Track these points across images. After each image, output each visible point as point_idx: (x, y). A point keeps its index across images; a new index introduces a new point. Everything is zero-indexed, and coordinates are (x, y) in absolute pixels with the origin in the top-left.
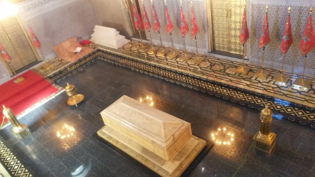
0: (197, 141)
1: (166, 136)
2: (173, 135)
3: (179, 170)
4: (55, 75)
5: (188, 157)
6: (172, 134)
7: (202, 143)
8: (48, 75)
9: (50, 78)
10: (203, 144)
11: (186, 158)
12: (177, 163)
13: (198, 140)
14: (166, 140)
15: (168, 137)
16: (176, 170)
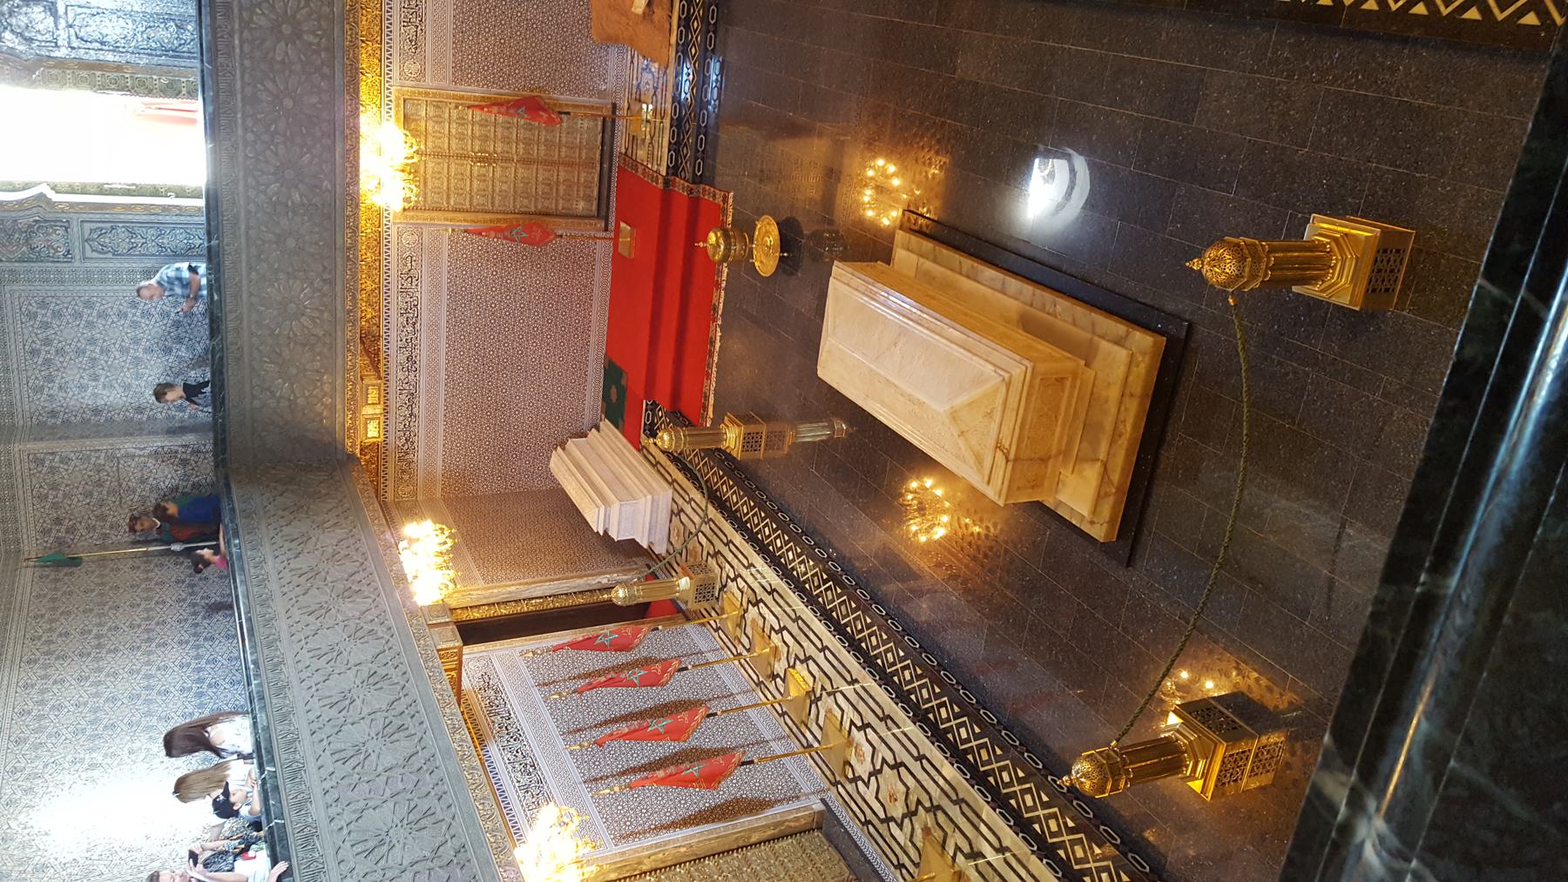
0: (1122, 354)
1: (979, 460)
2: (998, 446)
3: (1107, 495)
4: (676, 147)
5: (1116, 435)
6: (992, 443)
7: (1144, 354)
8: (663, 172)
9: (674, 170)
10: (1147, 359)
11: (1112, 443)
12: (1092, 473)
13: (1118, 342)
14: (987, 472)
15: (987, 464)
16: (1099, 497)
